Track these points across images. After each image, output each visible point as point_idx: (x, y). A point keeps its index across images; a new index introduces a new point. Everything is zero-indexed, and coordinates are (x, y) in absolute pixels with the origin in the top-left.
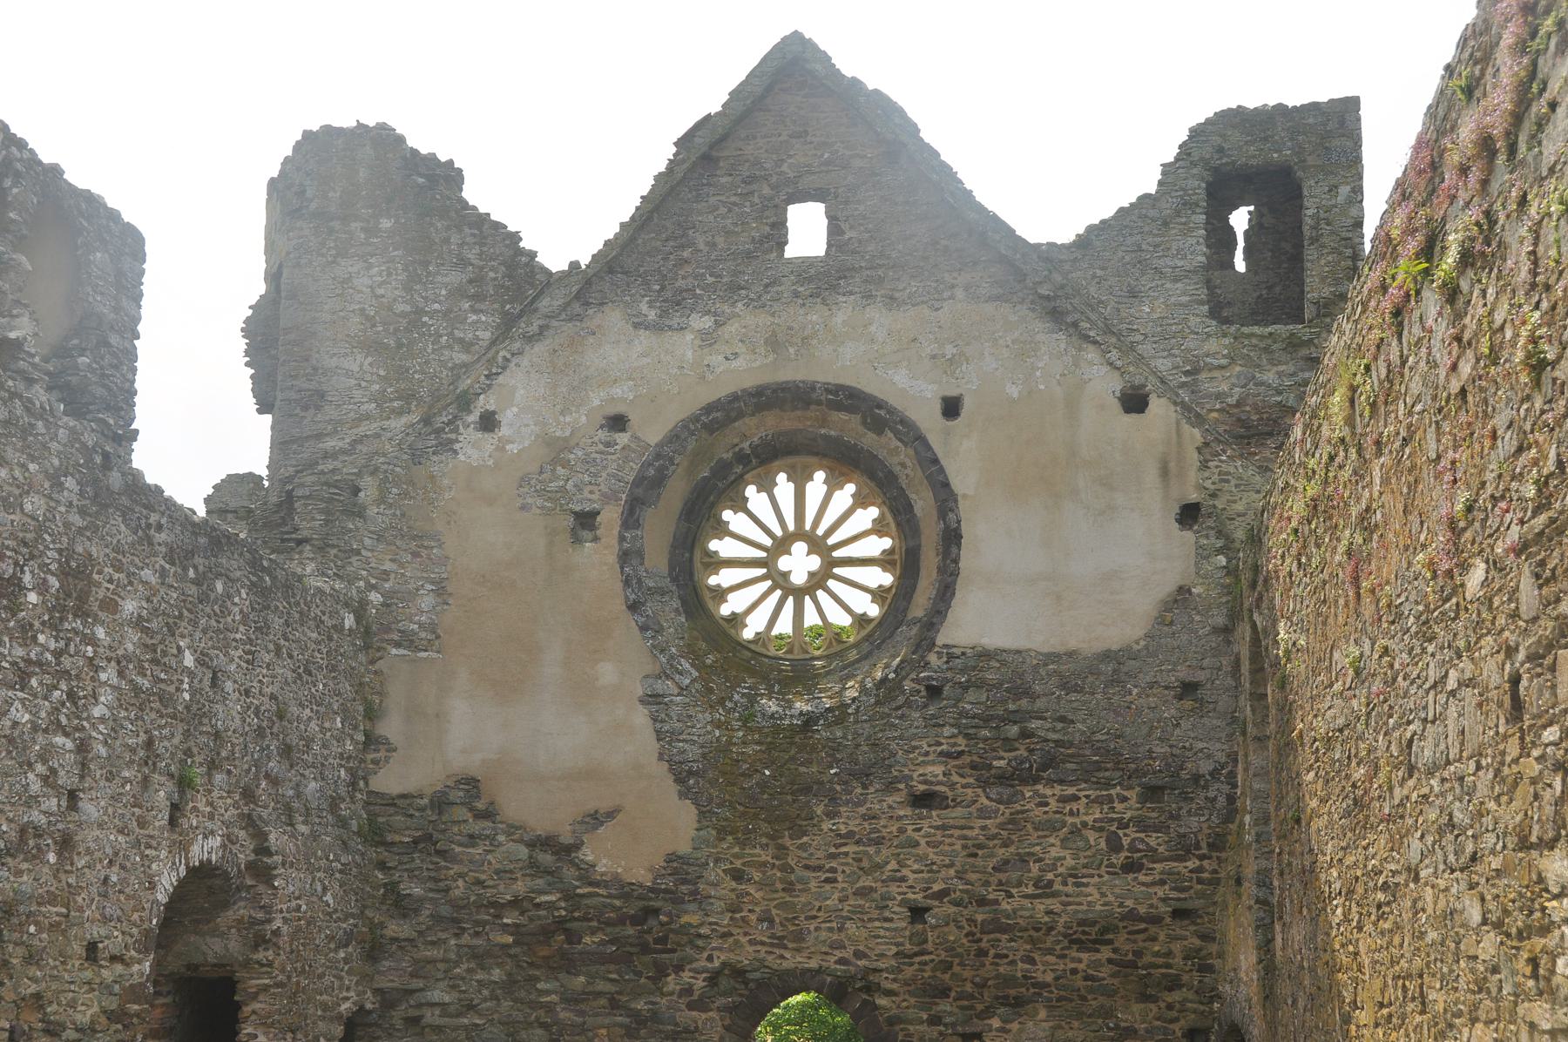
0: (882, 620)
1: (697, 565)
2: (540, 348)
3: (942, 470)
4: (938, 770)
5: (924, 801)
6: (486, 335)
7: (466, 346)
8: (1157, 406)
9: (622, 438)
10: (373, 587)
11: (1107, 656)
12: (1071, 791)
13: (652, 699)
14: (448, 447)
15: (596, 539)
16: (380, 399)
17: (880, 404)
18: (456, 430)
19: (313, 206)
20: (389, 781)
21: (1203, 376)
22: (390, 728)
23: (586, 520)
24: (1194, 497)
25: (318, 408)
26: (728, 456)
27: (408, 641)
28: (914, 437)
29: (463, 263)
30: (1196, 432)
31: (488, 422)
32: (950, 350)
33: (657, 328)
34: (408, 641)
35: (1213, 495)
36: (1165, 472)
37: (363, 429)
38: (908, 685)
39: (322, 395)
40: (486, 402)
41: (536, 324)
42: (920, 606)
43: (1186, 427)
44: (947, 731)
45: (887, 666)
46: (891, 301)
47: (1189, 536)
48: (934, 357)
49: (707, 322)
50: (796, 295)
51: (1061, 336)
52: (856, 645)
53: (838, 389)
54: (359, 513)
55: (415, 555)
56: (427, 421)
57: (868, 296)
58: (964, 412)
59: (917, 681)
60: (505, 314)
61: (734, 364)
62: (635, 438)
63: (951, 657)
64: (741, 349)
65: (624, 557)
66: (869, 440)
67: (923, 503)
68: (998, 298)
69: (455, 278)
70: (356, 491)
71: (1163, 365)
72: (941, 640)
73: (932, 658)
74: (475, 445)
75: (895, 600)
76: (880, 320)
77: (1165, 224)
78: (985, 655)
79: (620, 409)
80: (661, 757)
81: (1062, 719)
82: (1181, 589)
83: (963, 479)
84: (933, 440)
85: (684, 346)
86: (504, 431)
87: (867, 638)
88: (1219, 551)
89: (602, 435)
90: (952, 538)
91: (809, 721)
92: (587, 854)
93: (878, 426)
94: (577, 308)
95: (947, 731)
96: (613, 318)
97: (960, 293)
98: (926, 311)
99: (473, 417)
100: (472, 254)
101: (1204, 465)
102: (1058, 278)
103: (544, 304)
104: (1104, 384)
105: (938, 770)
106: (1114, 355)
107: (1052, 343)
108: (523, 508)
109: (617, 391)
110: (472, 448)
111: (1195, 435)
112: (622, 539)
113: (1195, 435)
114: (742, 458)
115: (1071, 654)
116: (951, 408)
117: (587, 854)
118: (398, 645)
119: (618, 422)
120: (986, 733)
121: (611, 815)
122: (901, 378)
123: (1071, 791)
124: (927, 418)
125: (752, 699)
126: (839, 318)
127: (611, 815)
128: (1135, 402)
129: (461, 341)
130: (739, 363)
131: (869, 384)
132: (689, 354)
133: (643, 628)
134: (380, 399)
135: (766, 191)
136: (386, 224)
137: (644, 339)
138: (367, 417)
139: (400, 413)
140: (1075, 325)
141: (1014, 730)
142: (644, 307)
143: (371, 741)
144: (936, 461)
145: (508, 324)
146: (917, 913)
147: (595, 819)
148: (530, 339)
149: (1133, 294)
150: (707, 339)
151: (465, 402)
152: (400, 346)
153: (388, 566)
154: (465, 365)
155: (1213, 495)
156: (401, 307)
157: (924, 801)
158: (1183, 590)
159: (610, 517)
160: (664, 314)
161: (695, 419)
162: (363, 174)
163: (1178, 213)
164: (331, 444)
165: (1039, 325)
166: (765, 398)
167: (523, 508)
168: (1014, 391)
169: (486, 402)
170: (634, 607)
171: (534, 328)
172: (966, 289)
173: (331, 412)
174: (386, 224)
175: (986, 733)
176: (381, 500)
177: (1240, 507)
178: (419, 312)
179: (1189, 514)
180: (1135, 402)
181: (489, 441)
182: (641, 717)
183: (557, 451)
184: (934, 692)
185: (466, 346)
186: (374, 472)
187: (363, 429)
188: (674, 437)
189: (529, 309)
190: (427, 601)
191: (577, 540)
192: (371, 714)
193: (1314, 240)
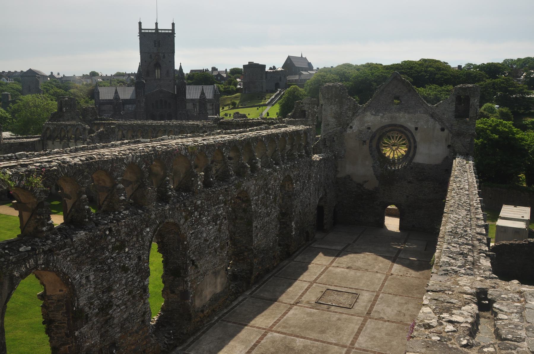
0: (405, 155)
1: (380, 146)
2: (358, 117)
3: (414, 138)
4: (412, 178)
5: (410, 182)
6: (351, 115)
7: (348, 117)
8: (446, 131)
9: (370, 131)
10: (336, 151)
11: (436, 165)
12: (429, 182)
13: (373, 167)
14: (345, 131)
15: (366, 144)
16: (336, 125)
17: (406, 128)
18: (347, 128)
19: (327, 97)
20: (339, 176)
21: (453, 126)
22: (339, 169)
23: (365, 142)
24: (450, 144)
25: (328, 126)
26: (384, 132)
27: (341, 158)
28: (410, 132)
29: (347, 105)
30: (451, 135)
31: (351, 127)
32: (417, 121)
33: (375, 115)
34: (341, 158)
35: (453, 144)
36: (446, 140)
37: (334, 129)
38: (408, 167)
39: (329, 124)
40: (351, 125)
41: (358, 114)
42: (411, 155)
43: (450, 134)
44: (413, 174)
45: (405, 164)
46: (409, 113)
47: (449, 149)
48: (414, 121)
49: (382, 115)
50: (395, 111)
51: (433, 119)
52: (401, 158)
53: (400, 125)
54: (334, 141)
55: (342, 146)
56: (343, 127)
57: (405, 112)
58: (418, 130)
59: (409, 166)
60: (353, 112)
61: (386, 121)
62: (371, 131)
63: (414, 164)
64: (386, 118)
65: (370, 147)
66: (405, 131)
67: (412, 140)
68: (424, 113)
69: (346, 107)
70: (334, 138)
71: (447, 125)
72: (413, 161)
73: (412, 163)
74: (349, 130)
75: (408, 152)
76: (407, 116)
77: (449, 104)
78: (419, 164)
79: (369, 126)
80: (374, 174)
81: (429, 173)
82: (447, 157)
83: (418, 139)
84: (414, 133)
85: (379, 118)
86: (353, 129)
87: (403, 157)
88: (453, 153)
89: (367, 130)
90: (415, 147)
91: (394, 170)
92: (364, 186)
93: (406, 130)
94: (363, 112)
95: (413, 174)
96: (369, 113)
97: (419, 112)
98: (413, 115)
99: (349, 127)
100: (349, 104)
101: (452, 139)
102: (433, 111)
103: (359, 111)
104: (438, 126)
105: (412, 178)
106: (440, 123)
107: (431, 120)
108: (356, 140)
109: (369, 124)
110: (349, 131)
111: (451, 135)
112: (369, 144)
113: (451, 135)
114: (387, 132)
115: (431, 165)
116: (416, 129)
117: (364, 186)
118: (339, 158)
119: (369, 128)
120: (418, 174)
121: (367, 181)
122: (409, 124)
123: (429, 182)
124: (413, 130)
125: (387, 167)
126: (401, 115)
127: (367, 181)
128: (443, 130)
129: (347, 116)
130: (386, 121)
131: (405, 125)
132: (379, 119)
133: (372, 157)
134: (336, 125)
135: (391, 95)
136: (337, 100)
137: (373, 117)
138: (335, 127)
139: (339, 127)
140: (435, 118)
141: (422, 174)
142: (373, 112)
143: (336, 171)
144: (414, 136)
145: (354, 114)
146: (407, 197)
147: (365, 182)
148: (357, 116)
149: (444, 114)
150: (382, 117)
151: (348, 125)
152: (339, 117)
153: (338, 148)
154: (348, 120)
155: (453, 144)
156: (339, 112)
157: (410, 182)
158: (447, 157)
159: (368, 141)
160: (376, 113)
161: (380, 128)
162: (334, 92)
163: (451, 102)
164: (330, 131)
165: (430, 118)
166: (389, 126)
167: (356, 140)
168: (425, 127)
169: (351, 125)
170: (371, 154)
171: (358, 115)
172: (420, 111)
173: (330, 127)
174: (337, 100)
175: (418, 174)
176: (337, 140)
177: (456, 146)
178: (342, 112)
179: (449, 146)
180: (443, 130)
181: (351, 130)
182: (372, 169)
183: (360, 132)
184: (412, 168)
185: (348, 117)
186: (336, 136)
187: (334, 129)
188: (377, 131)
189: (357, 112)
190: (343, 152)
191: (363, 144)
192: (336, 168)
193: (471, 107)
